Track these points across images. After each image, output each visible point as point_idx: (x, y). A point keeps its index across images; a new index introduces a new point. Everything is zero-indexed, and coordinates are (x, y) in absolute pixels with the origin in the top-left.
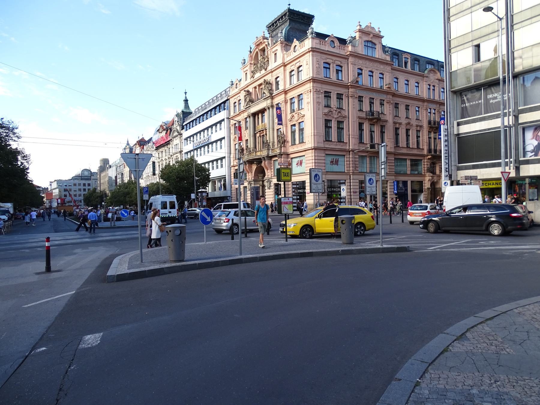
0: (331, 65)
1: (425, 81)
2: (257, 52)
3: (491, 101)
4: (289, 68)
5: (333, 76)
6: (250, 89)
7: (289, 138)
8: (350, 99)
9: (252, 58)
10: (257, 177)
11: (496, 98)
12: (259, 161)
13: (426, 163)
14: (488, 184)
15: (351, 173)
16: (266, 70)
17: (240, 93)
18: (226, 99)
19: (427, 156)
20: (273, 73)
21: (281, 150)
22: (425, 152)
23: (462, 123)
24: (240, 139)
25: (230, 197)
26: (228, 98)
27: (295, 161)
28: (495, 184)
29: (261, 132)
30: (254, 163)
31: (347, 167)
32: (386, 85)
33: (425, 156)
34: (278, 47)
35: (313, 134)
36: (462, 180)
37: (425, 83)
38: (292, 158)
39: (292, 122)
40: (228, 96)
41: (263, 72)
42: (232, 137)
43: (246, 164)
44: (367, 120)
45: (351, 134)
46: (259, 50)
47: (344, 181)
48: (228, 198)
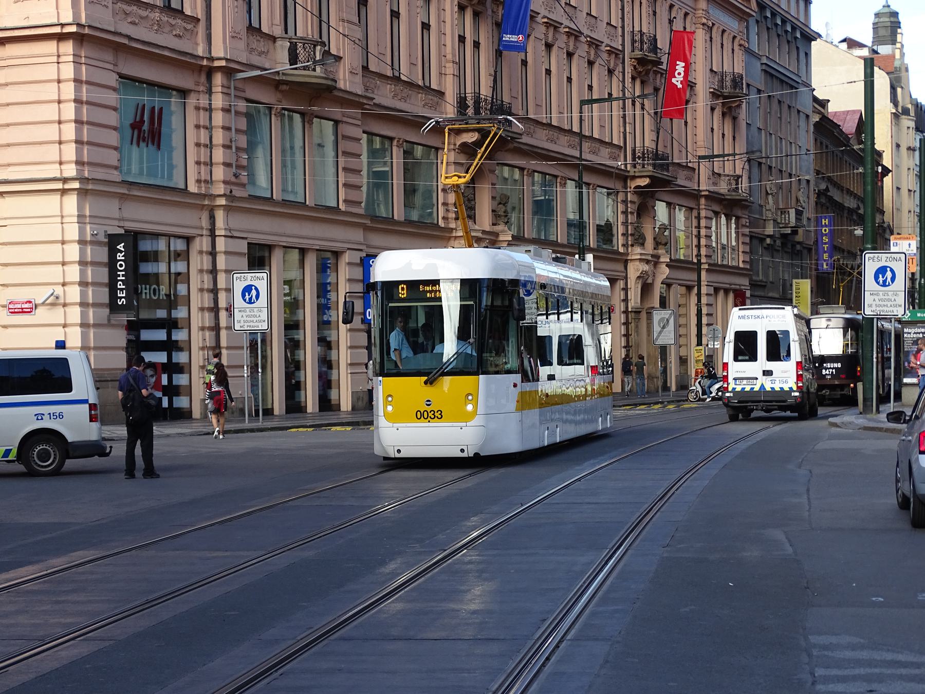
15: (222, 201)
31: (198, 163)
47: (179, 245)
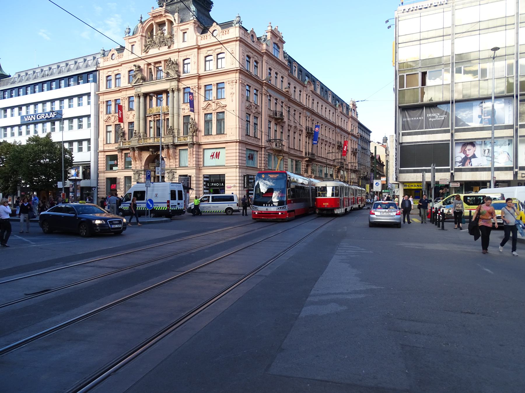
0: (251, 59)
1: (305, 91)
2: (152, 24)
3: (430, 119)
4: (204, 52)
5: (252, 70)
6: (142, 64)
7: (202, 127)
8: (263, 97)
9: (143, 29)
10: (147, 166)
11: (434, 117)
12: (156, 148)
13: (304, 165)
14: (410, 186)
16: (169, 47)
17: (121, 65)
18: (95, 69)
19: (305, 158)
20: (180, 53)
21: (193, 139)
22: (304, 155)
23: (407, 134)
24: (121, 120)
25: (95, 187)
26: (98, 69)
27: (208, 153)
28: (416, 186)
29: (158, 116)
30: (149, 151)
32: (285, 89)
33: (303, 158)
34: (190, 27)
35: (238, 126)
36: (441, 181)
37: (304, 92)
38: (204, 149)
39: (207, 111)
40: (97, 67)
41: (164, 49)
42: (103, 116)
43: (135, 151)
44: (274, 119)
45: (263, 131)
46: (155, 22)
48: (93, 189)
